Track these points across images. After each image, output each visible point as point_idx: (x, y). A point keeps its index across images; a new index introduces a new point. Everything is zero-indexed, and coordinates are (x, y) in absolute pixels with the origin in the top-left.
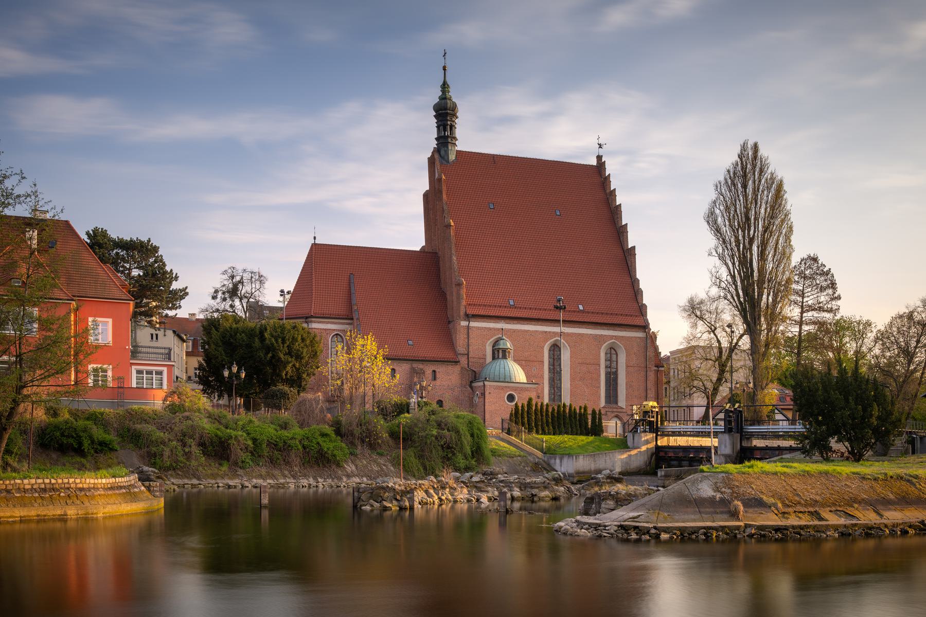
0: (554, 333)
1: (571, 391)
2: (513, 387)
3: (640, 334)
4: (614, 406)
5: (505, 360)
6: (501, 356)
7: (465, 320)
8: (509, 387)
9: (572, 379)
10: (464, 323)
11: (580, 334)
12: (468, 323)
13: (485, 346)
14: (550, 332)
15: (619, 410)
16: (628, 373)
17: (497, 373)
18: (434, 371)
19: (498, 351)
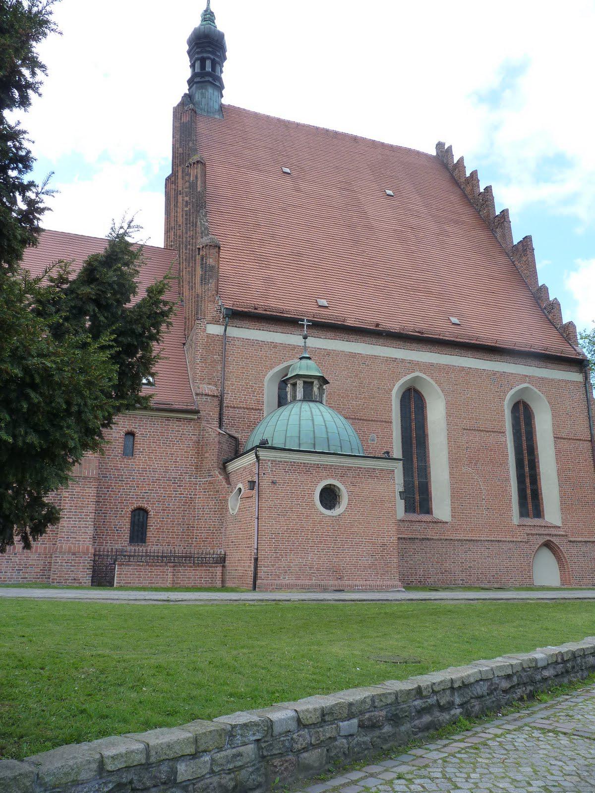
0: (411, 362)
1: (452, 489)
2: (336, 468)
3: (577, 377)
4: (536, 521)
5: (312, 404)
6: (300, 394)
7: (215, 322)
8: (325, 467)
9: (454, 462)
10: (215, 330)
11: (463, 369)
12: (223, 328)
13: (262, 382)
14: (403, 361)
15: (553, 531)
16: (558, 452)
17: (293, 432)
18: (131, 434)
19: (294, 385)
